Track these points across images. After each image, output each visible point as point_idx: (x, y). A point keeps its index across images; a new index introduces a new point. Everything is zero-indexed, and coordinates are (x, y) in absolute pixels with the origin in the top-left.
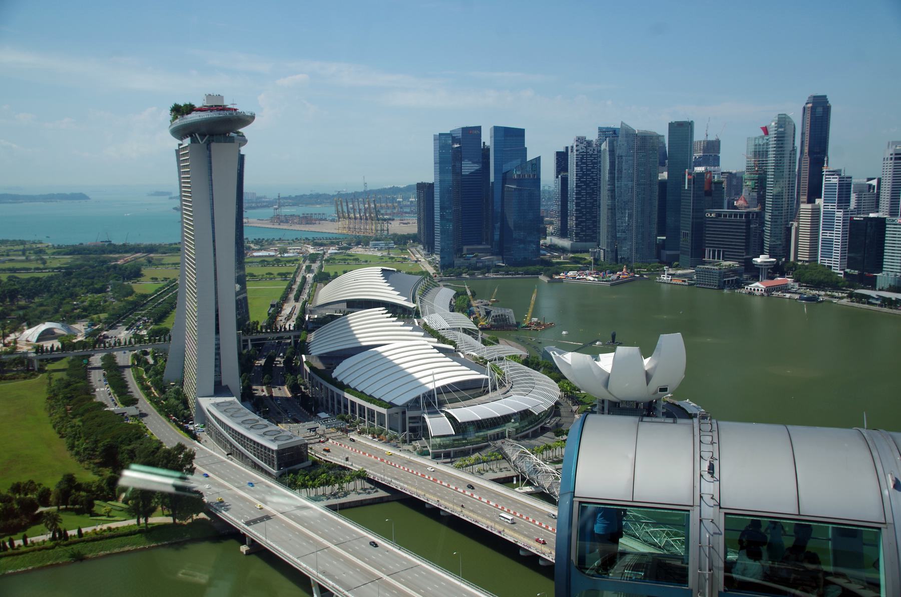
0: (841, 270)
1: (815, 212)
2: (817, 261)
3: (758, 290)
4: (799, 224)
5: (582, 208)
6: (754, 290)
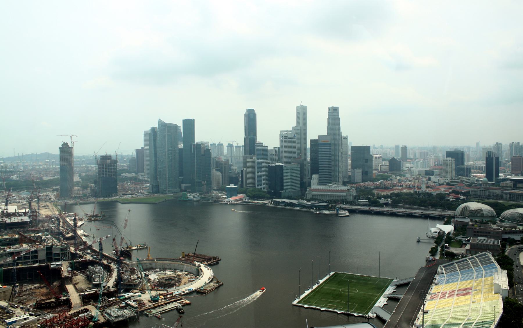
0: (266, 190)
1: (253, 162)
2: (256, 186)
3: (230, 202)
4: (246, 169)
6: (228, 202)
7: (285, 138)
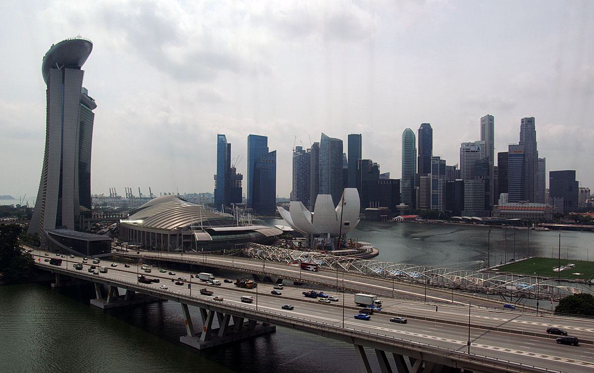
1: (428, 180)
5: (301, 187)
7: (467, 151)
